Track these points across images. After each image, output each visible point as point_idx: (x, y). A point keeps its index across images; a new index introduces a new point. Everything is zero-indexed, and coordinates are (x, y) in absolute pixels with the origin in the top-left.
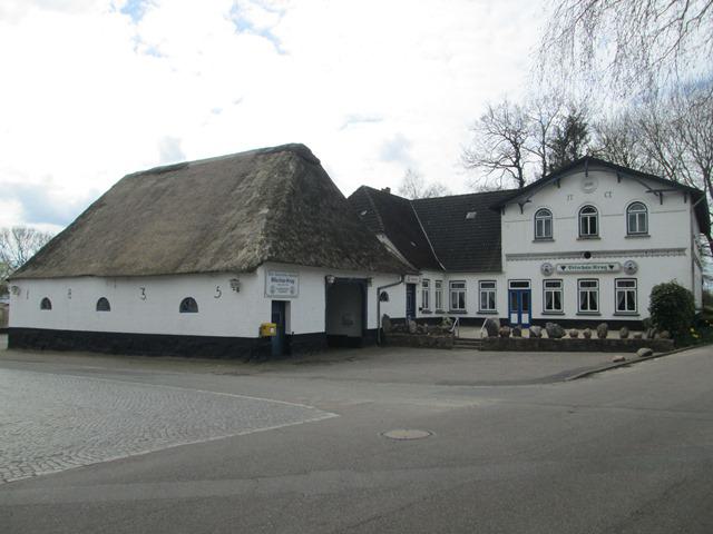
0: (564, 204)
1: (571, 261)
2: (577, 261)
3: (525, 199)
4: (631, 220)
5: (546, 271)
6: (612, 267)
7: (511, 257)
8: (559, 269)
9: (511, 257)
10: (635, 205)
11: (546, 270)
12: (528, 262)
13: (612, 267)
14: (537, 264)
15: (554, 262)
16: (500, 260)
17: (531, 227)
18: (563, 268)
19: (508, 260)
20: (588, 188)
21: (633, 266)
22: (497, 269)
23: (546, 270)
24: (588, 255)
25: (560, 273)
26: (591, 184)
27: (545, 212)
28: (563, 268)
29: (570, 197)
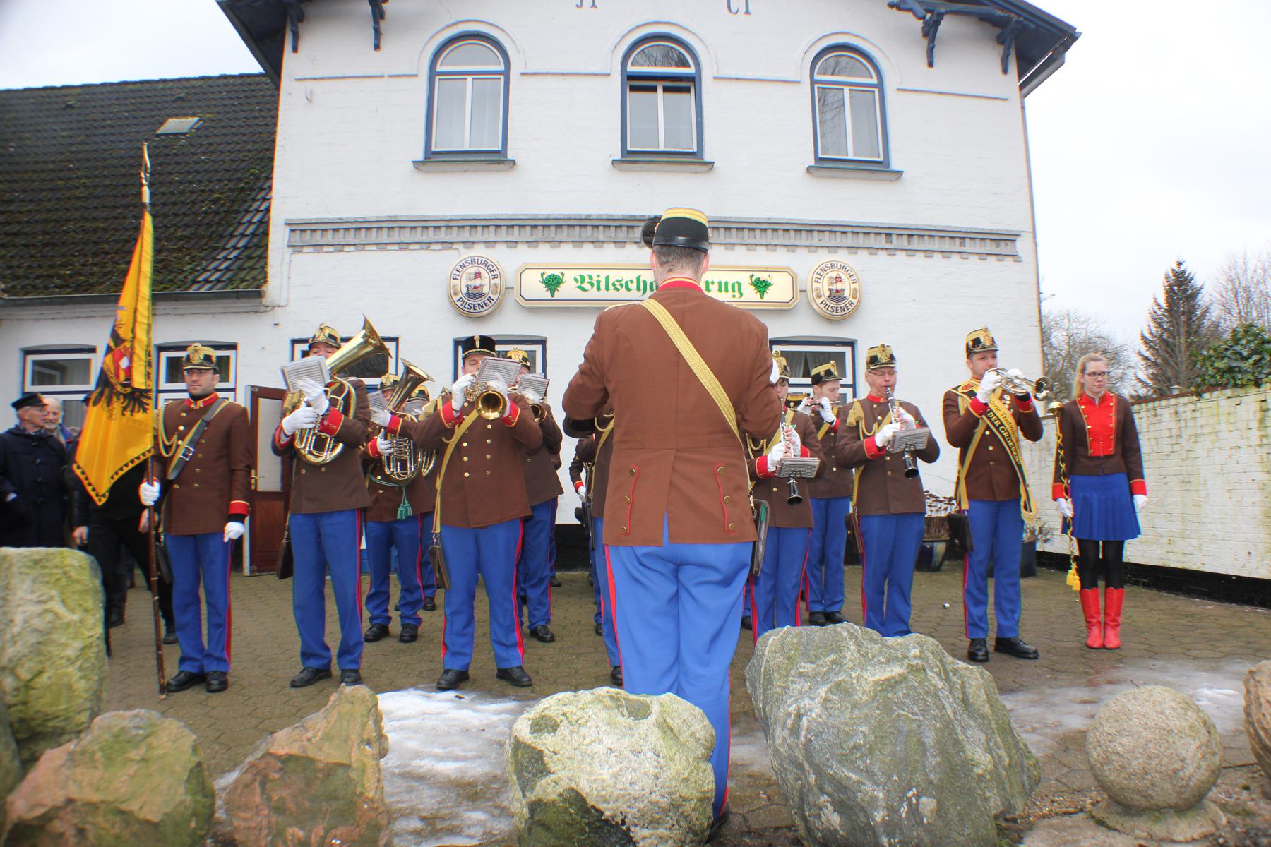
1: (588, 254)
2: (610, 253)
4: (824, 102)
5: (473, 302)
6: (761, 286)
7: (309, 234)
8: (534, 287)
9: (309, 234)
10: (839, 52)
11: (474, 294)
13: (761, 286)
14: (437, 268)
15: (524, 267)
16: (263, 257)
18: (553, 283)
19: (295, 247)
21: (847, 287)
22: (246, 284)
23: (474, 294)
25: (534, 309)
28: (553, 283)
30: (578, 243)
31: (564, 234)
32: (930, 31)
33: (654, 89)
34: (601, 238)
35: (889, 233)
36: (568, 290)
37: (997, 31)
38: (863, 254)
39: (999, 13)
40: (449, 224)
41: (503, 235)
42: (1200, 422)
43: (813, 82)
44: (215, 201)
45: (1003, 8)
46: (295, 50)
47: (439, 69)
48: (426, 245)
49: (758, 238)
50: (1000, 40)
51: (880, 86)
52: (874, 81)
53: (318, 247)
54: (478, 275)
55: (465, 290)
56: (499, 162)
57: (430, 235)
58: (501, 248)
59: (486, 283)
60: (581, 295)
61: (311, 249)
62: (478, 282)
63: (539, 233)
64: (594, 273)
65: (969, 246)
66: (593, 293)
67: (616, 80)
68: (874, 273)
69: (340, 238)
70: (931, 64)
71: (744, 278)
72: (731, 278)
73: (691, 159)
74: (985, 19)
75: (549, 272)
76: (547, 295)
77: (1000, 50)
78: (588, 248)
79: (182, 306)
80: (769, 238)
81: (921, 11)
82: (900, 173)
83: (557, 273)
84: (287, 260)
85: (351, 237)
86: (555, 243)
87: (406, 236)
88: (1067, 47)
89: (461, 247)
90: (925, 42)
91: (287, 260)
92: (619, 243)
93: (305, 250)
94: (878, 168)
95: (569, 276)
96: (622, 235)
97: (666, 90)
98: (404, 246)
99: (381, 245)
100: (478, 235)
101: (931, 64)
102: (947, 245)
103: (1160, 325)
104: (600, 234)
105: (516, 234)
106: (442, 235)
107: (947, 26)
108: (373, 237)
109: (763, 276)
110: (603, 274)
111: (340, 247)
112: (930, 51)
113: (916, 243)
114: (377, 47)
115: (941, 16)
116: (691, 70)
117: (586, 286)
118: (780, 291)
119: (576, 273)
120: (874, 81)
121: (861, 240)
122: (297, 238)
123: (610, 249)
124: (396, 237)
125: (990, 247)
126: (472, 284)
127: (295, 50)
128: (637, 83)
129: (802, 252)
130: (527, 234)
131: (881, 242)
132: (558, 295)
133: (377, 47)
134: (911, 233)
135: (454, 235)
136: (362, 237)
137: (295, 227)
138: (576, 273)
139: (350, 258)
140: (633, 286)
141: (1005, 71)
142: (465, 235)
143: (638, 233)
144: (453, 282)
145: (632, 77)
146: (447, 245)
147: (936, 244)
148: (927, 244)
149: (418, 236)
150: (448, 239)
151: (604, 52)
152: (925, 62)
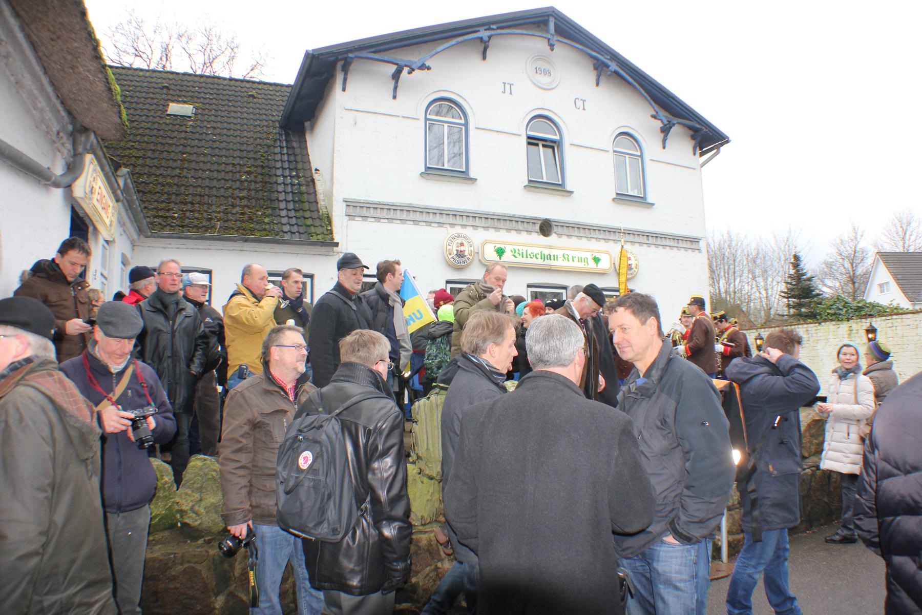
0: (501, 93)
2: (524, 237)
3: (413, 57)
6: (597, 260)
8: (490, 254)
12: (409, 228)
13: (597, 260)
17: (413, 136)
18: (500, 252)
19: (350, 216)
20: (543, 80)
23: (460, 254)
24: (546, 227)
26: (547, 73)
27: (447, 104)
28: (500, 252)
29: (507, 87)
30: (509, 230)
31: (502, 224)
32: (665, 130)
33: (537, 145)
34: (521, 228)
35: (648, 235)
36: (507, 257)
37: (691, 133)
38: (637, 245)
39: (698, 126)
40: (441, 212)
41: (471, 222)
42: (819, 334)
43: (614, 151)
44: (249, 173)
45: (700, 124)
46: (344, 90)
47: (429, 117)
48: (429, 223)
49: (593, 234)
50: (693, 137)
51: (641, 156)
52: (639, 153)
53: (365, 218)
54: (462, 244)
55: (455, 252)
56: (465, 179)
57: (431, 218)
58: (470, 229)
59: (466, 249)
60: (514, 260)
61: (373, 220)
62: (462, 248)
63: (490, 223)
64: (521, 248)
65: (681, 244)
66: (519, 259)
67: (524, 140)
68: (640, 254)
69: (378, 213)
70: (664, 148)
71: (589, 256)
72: (583, 255)
73: (558, 188)
74: (690, 128)
75: (498, 246)
76: (497, 259)
77: (692, 143)
78: (514, 233)
79: (277, 247)
80: (597, 235)
81: (666, 122)
82: (653, 204)
83: (502, 246)
84: (345, 224)
85: (385, 214)
86: (497, 229)
87: (418, 217)
88: (722, 145)
89: (448, 226)
90: (662, 135)
91: (345, 224)
92: (529, 232)
93: (357, 219)
94: (641, 201)
95: (508, 249)
96: (530, 227)
97: (544, 146)
98: (416, 222)
99: (402, 221)
100: (458, 220)
101: (664, 148)
102: (672, 243)
103: (818, 295)
104: (520, 226)
105: (477, 222)
106: (438, 218)
107: (676, 129)
108: (398, 215)
109: (597, 255)
110: (525, 249)
111: (378, 219)
112: (664, 141)
113: (659, 242)
114: (394, 97)
115: (674, 124)
116: (557, 138)
117: (516, 255)
118: (605, 264)
119: (512, 247)
120: (639, 153)
121: (636, 239)
122: (351, 211)
123: (524, 234)
124: (412, 216)
125: (689, 245)
126: (459, 249)
127: (344, 90)
128: (532, 141)
129: (611, 243)
130: (483, 223)
131: (644, 240)
132: (503, 259)
133: (394, 97)
134: (658, 236)
135: (444, 219)
136: (392, 215)
137: (349, 203)
138: (512, 247)
139: (384, 226)
140: (539, 256)
141: (695, 154)
142: (451, 220)
143: (537, 227)
144: (449, 247)
145: (529, 138)
146: (440, 224)
147: (668, 242)
148: (664, 242)
149: (425, 217)
150: (441, 221)
151: (518, 125)
152: (661, 146)
